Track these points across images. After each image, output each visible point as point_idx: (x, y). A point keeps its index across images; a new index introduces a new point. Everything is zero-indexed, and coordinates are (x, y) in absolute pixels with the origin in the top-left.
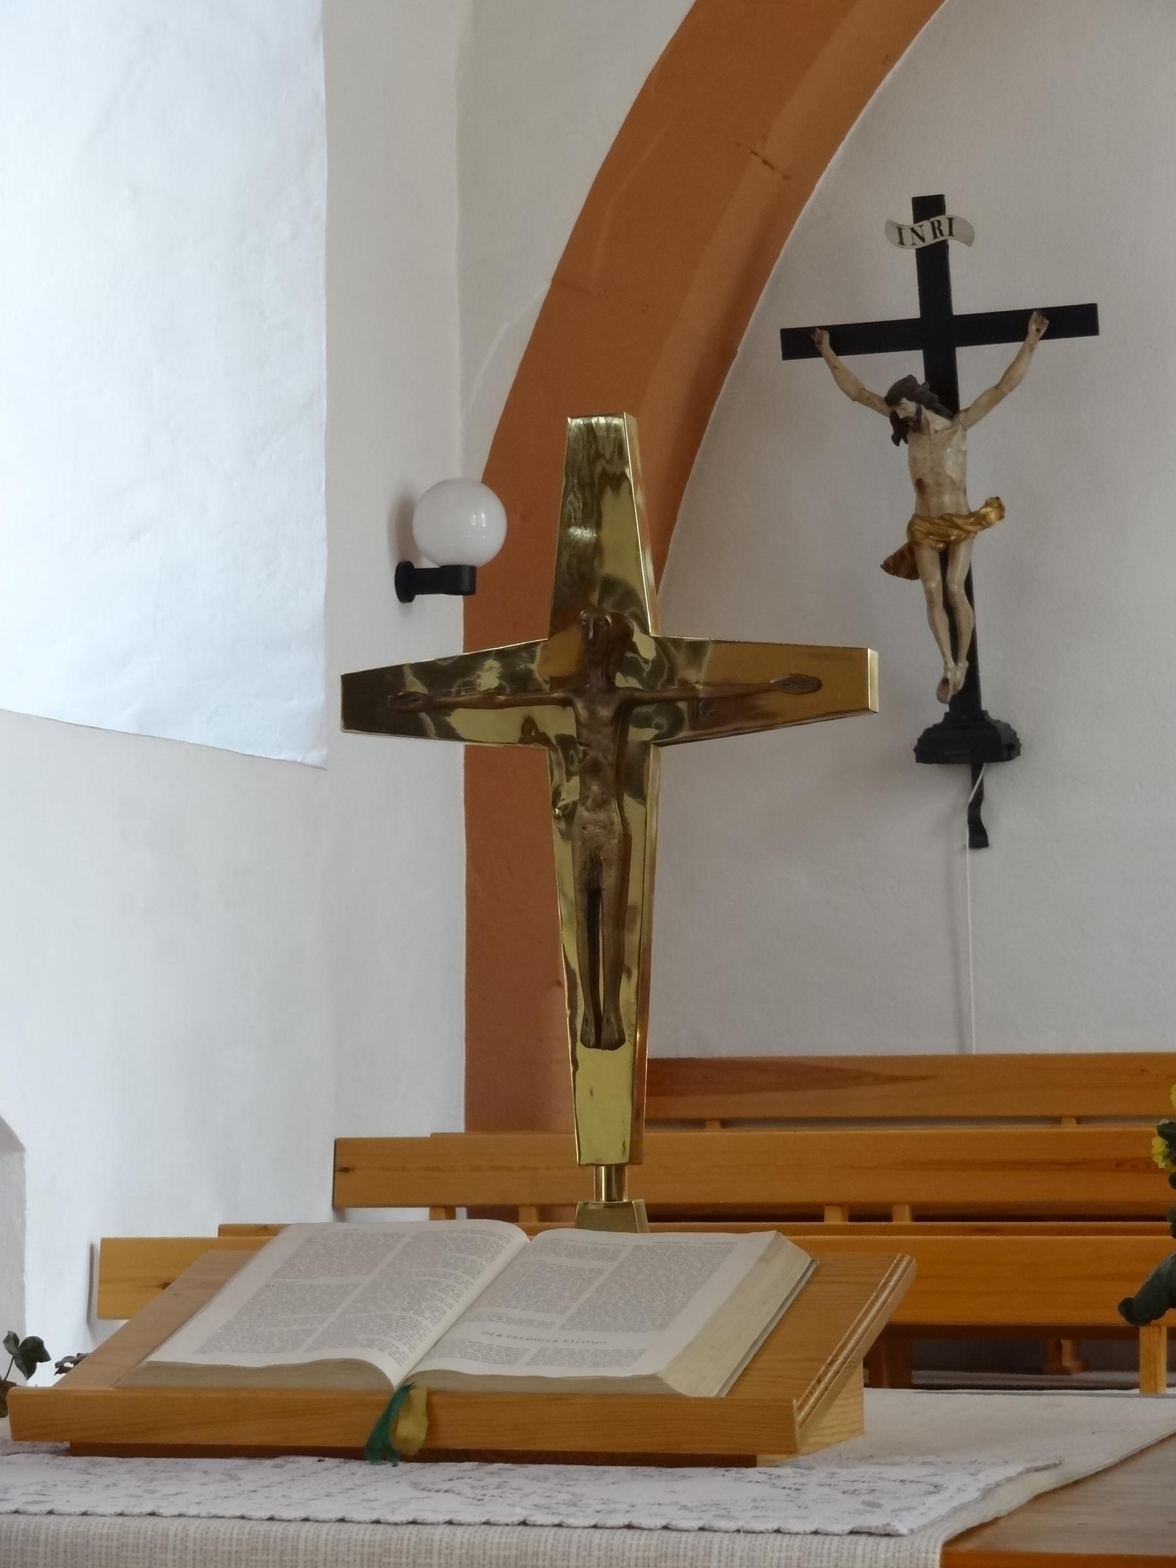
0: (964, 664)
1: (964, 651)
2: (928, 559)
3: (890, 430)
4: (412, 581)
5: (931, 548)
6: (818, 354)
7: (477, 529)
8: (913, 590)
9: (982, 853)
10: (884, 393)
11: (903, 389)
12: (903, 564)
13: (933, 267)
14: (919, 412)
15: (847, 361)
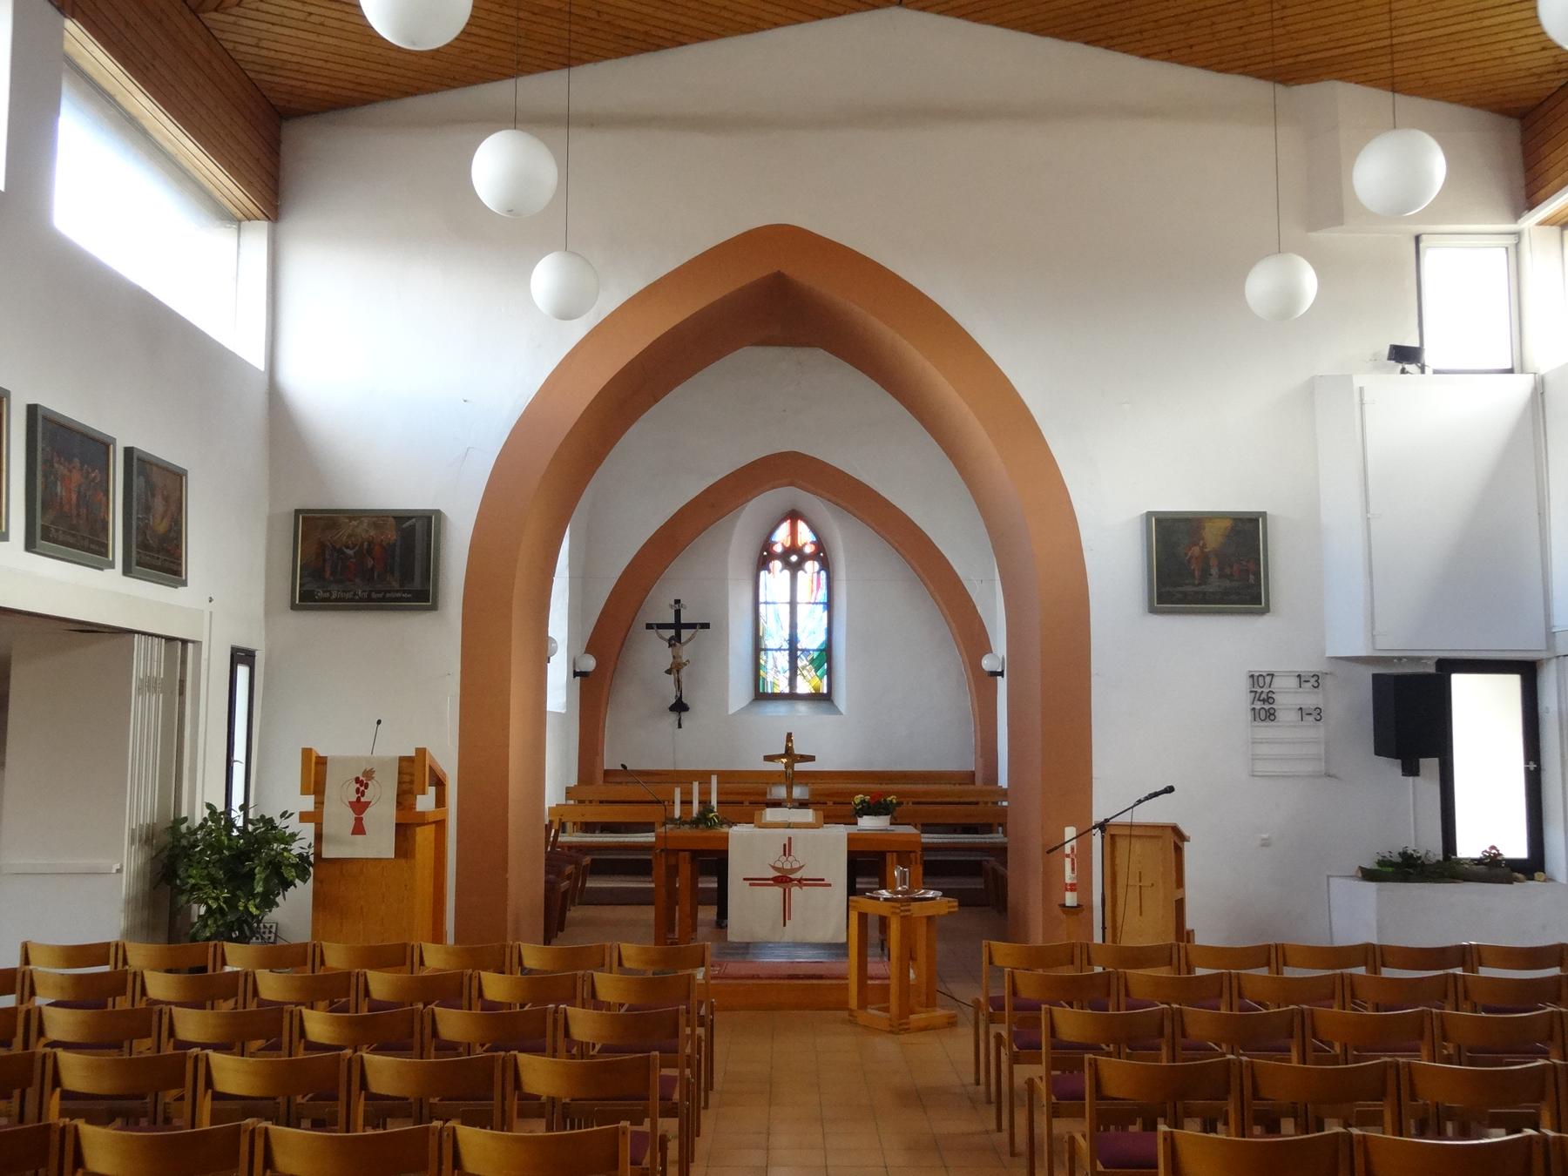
4: (576, 674)
5: (675, 669)
7: (589, 664)
8: (671, 678)
12: (669, 672)
13: (678, 613)
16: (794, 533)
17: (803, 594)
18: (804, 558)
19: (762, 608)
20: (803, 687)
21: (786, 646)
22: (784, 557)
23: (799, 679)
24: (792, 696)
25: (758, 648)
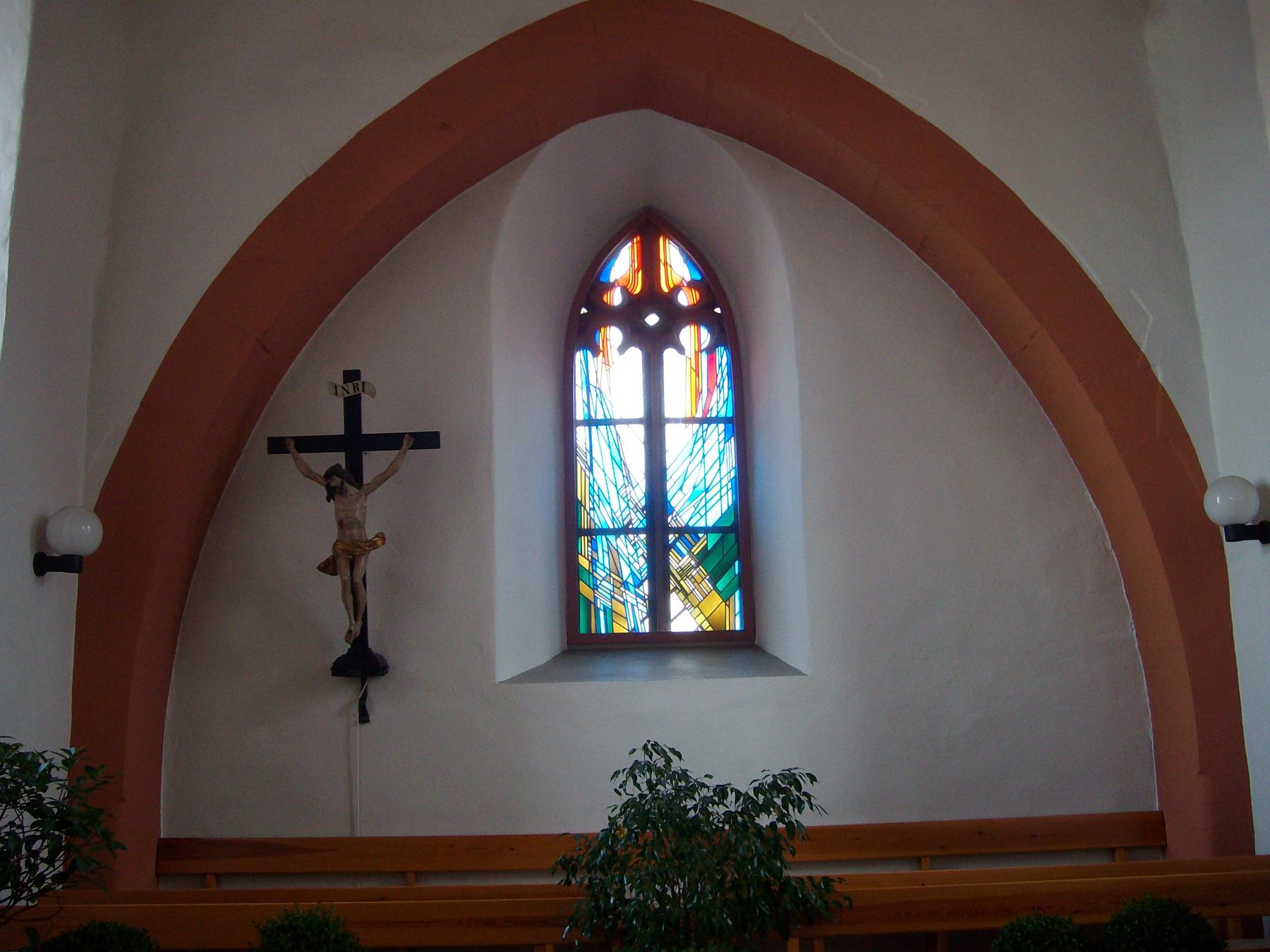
0: (360, 623)
1: (361, 616)
2: (343, 564)
3: (324, 492)
4: (44, 563)
5: (346, 559)
6: (287, 452)
7: (83, 534)
9: (366, 726)
10: (323, 474)
11: (334, 471)
12: (329, 567)
13: (353, 408)
14: (342, 484)
15: (304, 456)
16: (649, 263)
17: (677, 400)
18: (675, 317)
19: (581, 434)
20: (684, 620)
21: (638, 520)
22: (629, 317)
23: (675, 602)
24: (658, 642)
25: (571, 527)
